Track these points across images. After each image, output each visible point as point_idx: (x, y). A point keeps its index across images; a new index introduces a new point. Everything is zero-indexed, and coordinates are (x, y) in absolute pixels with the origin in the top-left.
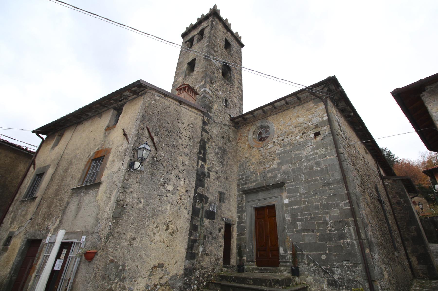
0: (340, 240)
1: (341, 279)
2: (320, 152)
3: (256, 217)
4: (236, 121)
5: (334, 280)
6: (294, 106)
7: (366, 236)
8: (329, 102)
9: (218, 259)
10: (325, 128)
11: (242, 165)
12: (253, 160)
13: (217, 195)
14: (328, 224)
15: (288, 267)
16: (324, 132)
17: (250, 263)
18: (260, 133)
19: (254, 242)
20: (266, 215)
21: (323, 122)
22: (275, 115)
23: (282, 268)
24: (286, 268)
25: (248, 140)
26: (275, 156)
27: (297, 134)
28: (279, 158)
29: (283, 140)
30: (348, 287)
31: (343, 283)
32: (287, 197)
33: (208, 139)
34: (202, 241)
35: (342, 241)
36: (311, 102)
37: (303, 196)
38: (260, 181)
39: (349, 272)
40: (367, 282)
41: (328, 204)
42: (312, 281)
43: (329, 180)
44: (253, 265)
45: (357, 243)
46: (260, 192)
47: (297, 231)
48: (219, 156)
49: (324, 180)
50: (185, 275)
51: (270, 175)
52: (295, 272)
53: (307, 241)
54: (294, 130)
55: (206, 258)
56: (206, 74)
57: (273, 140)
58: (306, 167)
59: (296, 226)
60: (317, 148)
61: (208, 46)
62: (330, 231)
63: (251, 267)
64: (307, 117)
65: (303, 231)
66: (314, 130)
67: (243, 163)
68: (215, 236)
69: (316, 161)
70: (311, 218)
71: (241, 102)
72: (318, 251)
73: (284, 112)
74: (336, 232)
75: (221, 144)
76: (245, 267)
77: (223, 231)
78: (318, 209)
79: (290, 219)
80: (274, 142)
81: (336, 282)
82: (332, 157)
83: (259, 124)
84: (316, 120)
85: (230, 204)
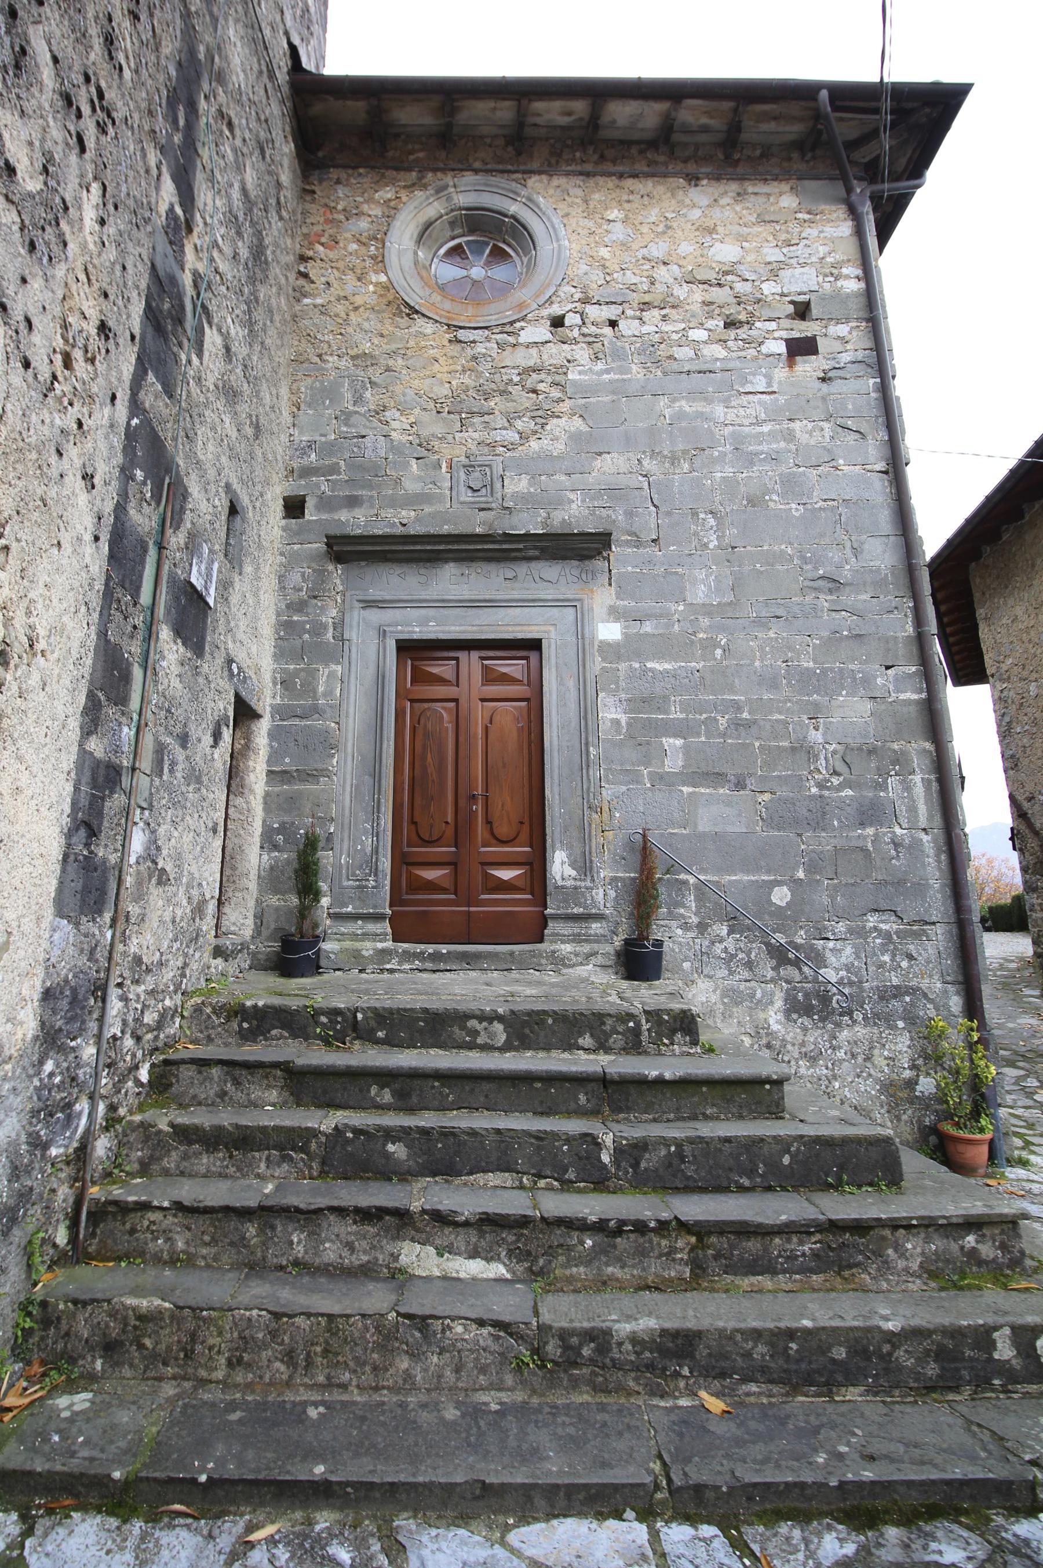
0: (862, 825)
1: (851, 984)
2: (810, 433)
4: (317, 108)
6: (691, 167)
10: (842, 330)
14: (816, 757)
15: (598, 939)
16: (837, 346)
17: (358, 927)
21: (838, 297)
22: (579, 180)
23: (567, 948)
24: (586, 948)
25: (380, 261)
26: (556, 393)
30: (876, 1015)
32: (615, 614)
35: (870, 831)
36: (785, 187)
37: (705, 622)
39: (886, 958)
40: (958, 993)
41: (824, 671)
42: (714, 998)
44: (375, 937)
45: (935, 841)
46: (452, 564)
47: (660, 779)
52: (639, 961)
53: (704, 825)
54: (681, 292)
57: (556, 310)
58: (730, 485)
59: (651, 754)
62: (820, 786)
63: (368, 948)
64: (758, 250)
66: (786, 323)
70: (738, 724)
72: (758, 869)
73: (629, 183)
74: (849, 792)
76: (327, 946)
78: (774, 686)
79: (623, 719)
80: (558, 322)
81: (825, 999)
83: (469, 191)
84: (801, 281)
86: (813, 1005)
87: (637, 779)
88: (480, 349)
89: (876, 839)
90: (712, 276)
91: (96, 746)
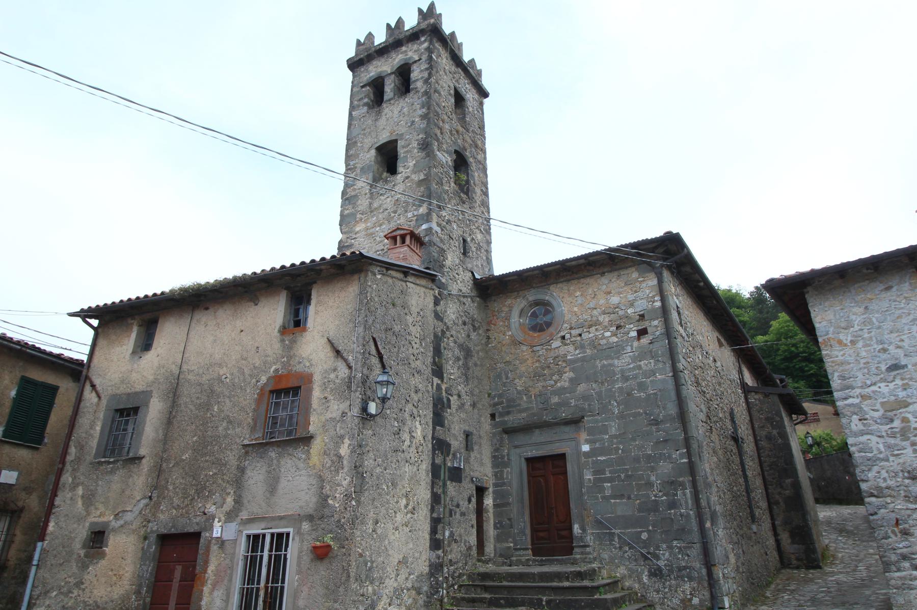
3: (529, 475)
5: (659, 569)
7: (708, 503)
8: (666, 274)
9: (470, 548)
10: (656, 323)
11: (499, 376)
12: (523, 369)
13: (461, 438)
16: (655, 329)
17: (522, 552)
18: (534, 315)
19: (527, 518)
20: (548, 472)
21: (654, 310)
22: (565, 284)
23: (578, 556)
25: (509, 327)
26: (564, 365)
27: (606, 327)
28: (573, 370)
29: (580, 335)
30: (678, 577)
31: (671, 571)
32: (587, 442)
33: (443, 332)
34: (447, 519)
36: (633, 269)
37: (615, 441)
38: (535, 410)
43: (659, 415)
44: (528, 555)
47: (604, 498)
48: (461, 363)
49: (651, 415)
50: (431, 574)
51: (555, 400)
53: (619, 513)
54: (601, 319)
55: (454, 546)
56: (429, 189)
57: (562, 334)
59: (602, 489)
60: (641, 357)
61: (424, 117)
62: (655, 496)
63: (523, 559)
65: (615, 497)
67: (500, 373)
68: (463, 509)
69: (638, 380)
70: (627, 476)
71: (488, 237)
75: (462, 337)
77: (474, 500)
80: (563, 338)
82: (664, 376)
84: (641, 305)
85: (481, 453)
86: (656, 573)
87: (597, 498)
88: (541, 353)
89: (675, 514)
90: (611, 310)
91: (435, 515)
